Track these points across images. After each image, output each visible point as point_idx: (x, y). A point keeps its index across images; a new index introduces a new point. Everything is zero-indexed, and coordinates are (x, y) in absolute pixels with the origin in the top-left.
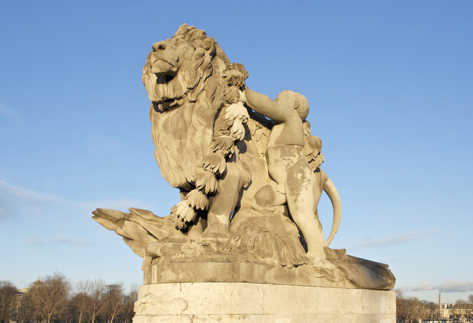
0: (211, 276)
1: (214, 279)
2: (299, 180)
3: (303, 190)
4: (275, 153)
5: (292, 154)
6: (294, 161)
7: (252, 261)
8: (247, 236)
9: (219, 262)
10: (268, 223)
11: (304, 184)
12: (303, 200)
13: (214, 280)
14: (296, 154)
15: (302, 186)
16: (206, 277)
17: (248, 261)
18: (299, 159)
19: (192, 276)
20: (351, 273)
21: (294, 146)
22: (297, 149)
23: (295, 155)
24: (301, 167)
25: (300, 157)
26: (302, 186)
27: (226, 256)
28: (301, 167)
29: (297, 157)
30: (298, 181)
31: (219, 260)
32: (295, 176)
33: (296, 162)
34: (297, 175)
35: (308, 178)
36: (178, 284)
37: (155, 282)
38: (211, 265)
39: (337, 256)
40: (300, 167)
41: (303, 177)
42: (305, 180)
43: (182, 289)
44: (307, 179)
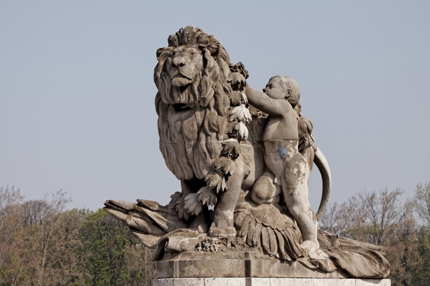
0: (228, 272)
1: (231, 274)
2: (295, 175)
3: (299, 184)
4: (272, 147)
5: (288, 149)
6: (290, 156)
7: (258, 256)
8: (251, 231)
9: (234, 259)
10: (268, 217)
11: (299, 179)
12: (299, 194)
13: (231, 276)
14: (292, 149)
15: (298, 181)
16: (225, 273)
17: (256, 257)
18: (294, 154)
19: (213, 272)
20: (343, 263)
21: (289, 142)
22: (292, 143)
23: (290, 150)
24: (297, 163)
25: (295, 152)
26: (298, 181)
27: (238, 252)
28: (297, 163)
29: (293, 153)
30: (295, 176)
31: (233, 257)
32: (292, 171)
33: (292, 157)
34: (293, 170)
35: (303, 173)
36: (202, 279)
37: (178, 276)
38: (227, 262)
39: (329, 242)
40: (296, 161)
41: (299, 172)
42: (301, 175)
43: (206, 284)
44: (302, 174)
